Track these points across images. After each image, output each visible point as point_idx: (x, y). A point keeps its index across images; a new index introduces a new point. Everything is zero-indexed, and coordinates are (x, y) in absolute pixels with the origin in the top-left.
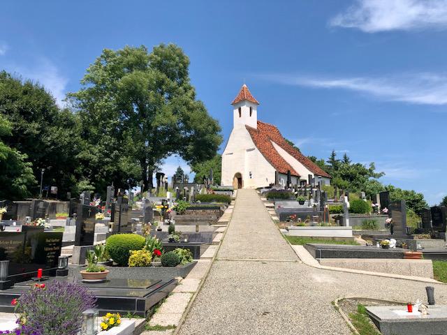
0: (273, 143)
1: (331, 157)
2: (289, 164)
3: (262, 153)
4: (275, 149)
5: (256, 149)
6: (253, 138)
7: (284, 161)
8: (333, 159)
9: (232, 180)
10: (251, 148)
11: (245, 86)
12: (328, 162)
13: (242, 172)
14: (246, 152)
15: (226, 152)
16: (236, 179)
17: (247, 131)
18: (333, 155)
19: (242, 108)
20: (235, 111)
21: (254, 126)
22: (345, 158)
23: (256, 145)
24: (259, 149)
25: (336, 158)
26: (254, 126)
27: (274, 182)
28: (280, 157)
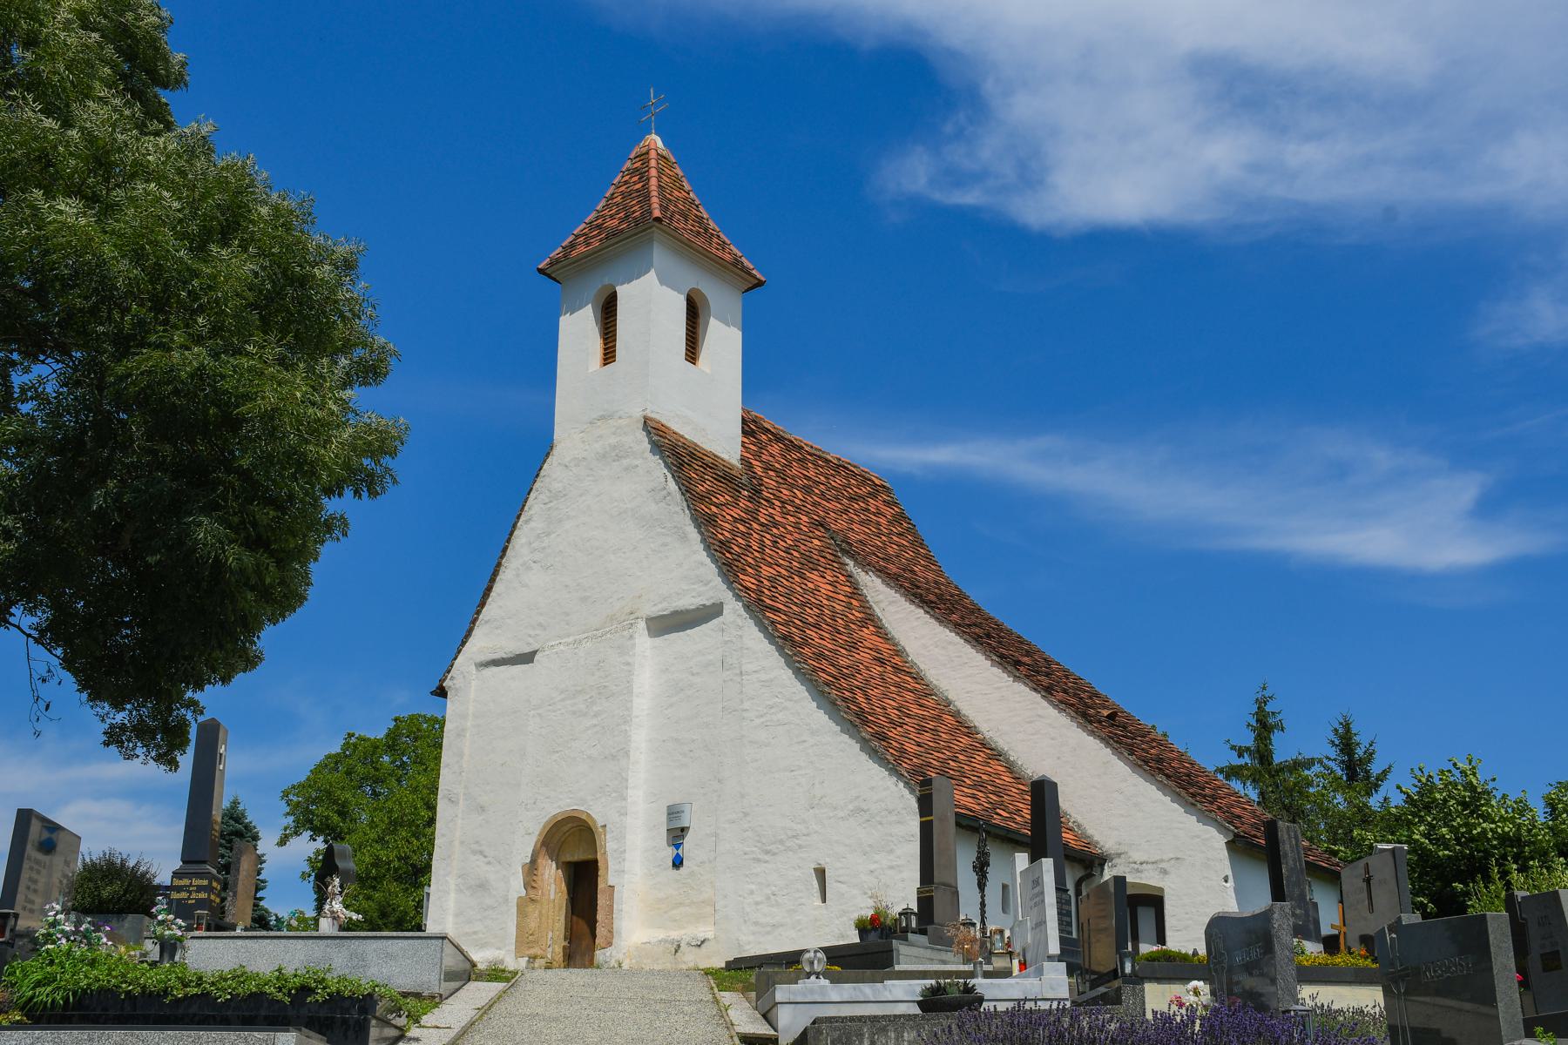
0: (877, 591)
1: (1248, 740)
2: (996, 755)
3: (788, 643)
4: (882, 633)
5: (734, 608)
6: (705, 522)
7: (964, 727)
8: (1263, 754)
9: (517, 887)
10: (689, 601)
11: (656, 141)
12: (1232, 772)
13: (598, 813)
14: (643, 641)
15: (481, 643)
16: (552, 878)
17: (656, 470)
18: (1264, 726)
19: (618, 289)
20: (566, 322)
21: (725, 443)
22: (1346, 742)
23: (730, 569)
24: (757, 607)
25: (1283, 750)
26: (725, 443)
27: (902, 895)
28: (924, 691)
